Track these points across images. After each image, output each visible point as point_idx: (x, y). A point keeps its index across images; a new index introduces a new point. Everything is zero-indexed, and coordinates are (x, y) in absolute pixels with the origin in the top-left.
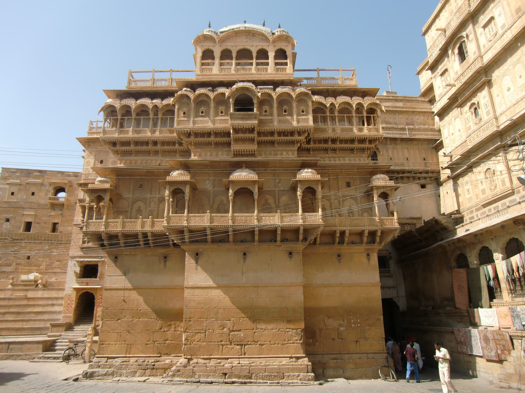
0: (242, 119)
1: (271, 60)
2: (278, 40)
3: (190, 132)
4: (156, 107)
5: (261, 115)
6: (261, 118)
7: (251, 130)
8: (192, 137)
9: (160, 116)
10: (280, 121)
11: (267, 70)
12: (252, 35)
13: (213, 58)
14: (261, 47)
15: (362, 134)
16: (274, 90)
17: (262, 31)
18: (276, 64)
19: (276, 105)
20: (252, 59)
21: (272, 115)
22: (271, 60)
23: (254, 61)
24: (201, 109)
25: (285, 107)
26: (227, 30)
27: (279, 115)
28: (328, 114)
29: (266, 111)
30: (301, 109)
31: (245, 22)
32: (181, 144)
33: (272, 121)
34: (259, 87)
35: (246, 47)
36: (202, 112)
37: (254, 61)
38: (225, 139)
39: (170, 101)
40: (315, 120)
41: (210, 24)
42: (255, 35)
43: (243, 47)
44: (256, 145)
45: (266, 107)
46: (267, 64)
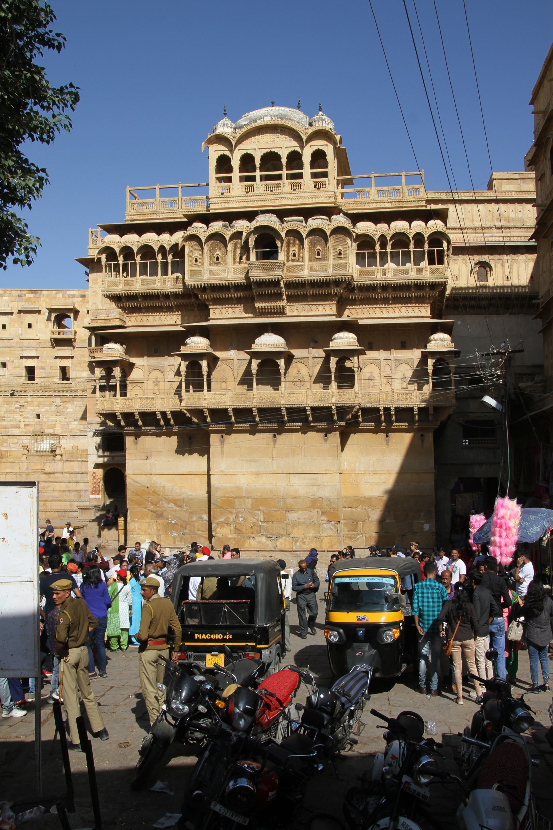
0: (264, 268)
1: (307, 171)
2: (315, 136)
3: (205, 286)
4: (162, 249)
5: (288, 260)
6: (287, 264)
7: (276, 283)
8: (208, 291)
9: (170, 258)
10: (312, 268)
11: (301, 186)
12: (281, 130)
13: (230, 170)
14: (292, 149)
15: (420, 276)
16: (306, 223)
17: (295, 121)
18: (314, 175)
19: (307, 246)
20: (282, 170)
21: (301, 260)
22: (307, 171)
23: (284, 172)
24: (216, 253)
25: (318, 247)
26: (246, 123)
27: (311, 260)
28: (378, 249)
29: (294, 255)
30: (338, 249)
31: (273, 104)
32: (196, 297)
33: (301, 268)
34: (286, 219)
35: (272, 150)
36: (218, 259)
37: (284, 172)
38: (247, 293)
39: (179, 236)
40: (360, 258)
41: (225, 110)
42: (285, 129)
43: (268, 150)
44: (283, 300)
45: (294, 249)
46: (300, 176)
